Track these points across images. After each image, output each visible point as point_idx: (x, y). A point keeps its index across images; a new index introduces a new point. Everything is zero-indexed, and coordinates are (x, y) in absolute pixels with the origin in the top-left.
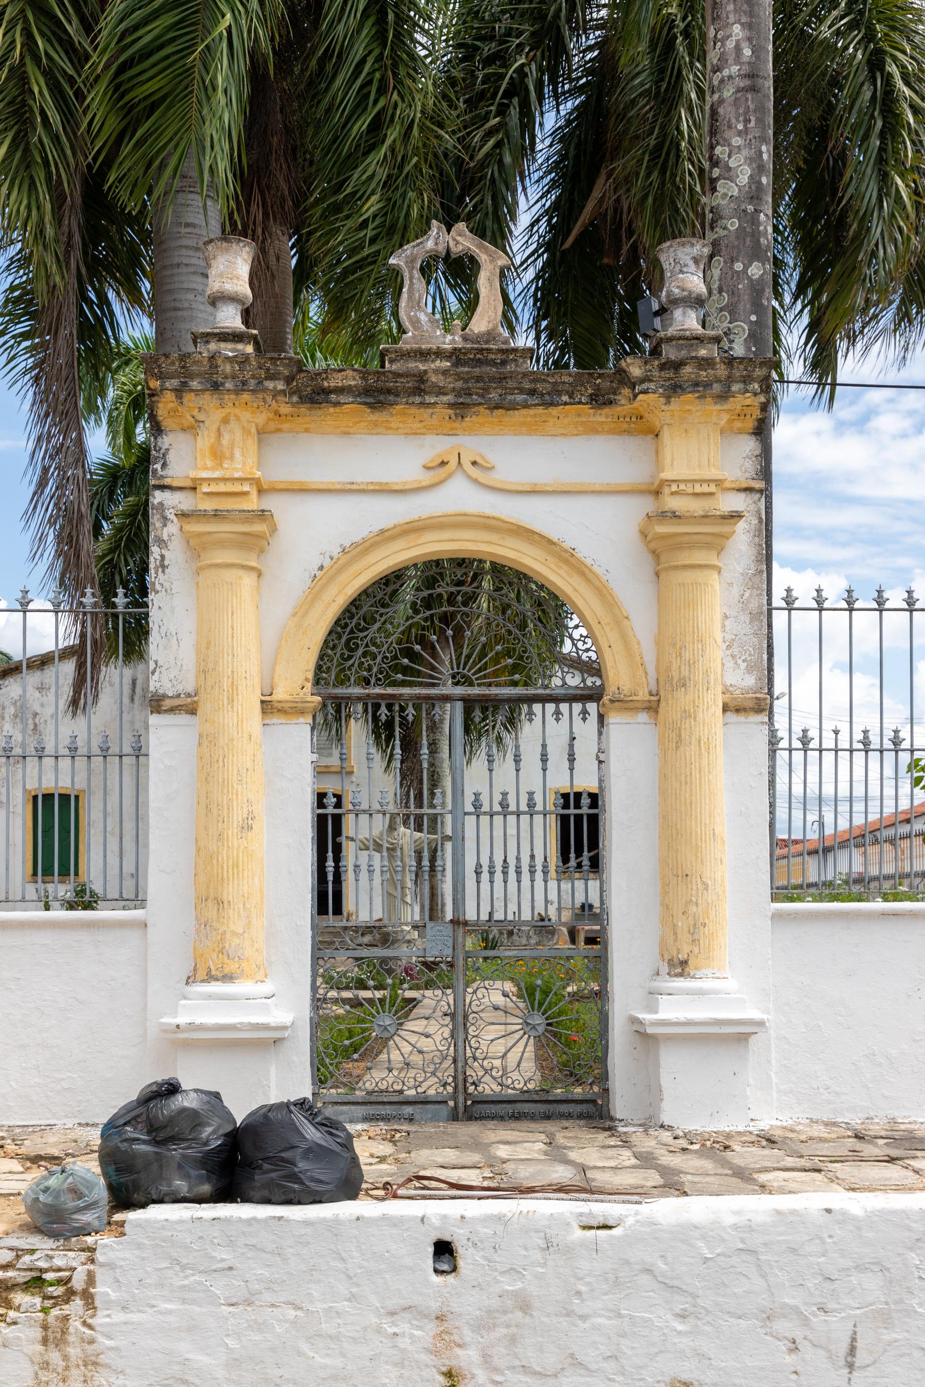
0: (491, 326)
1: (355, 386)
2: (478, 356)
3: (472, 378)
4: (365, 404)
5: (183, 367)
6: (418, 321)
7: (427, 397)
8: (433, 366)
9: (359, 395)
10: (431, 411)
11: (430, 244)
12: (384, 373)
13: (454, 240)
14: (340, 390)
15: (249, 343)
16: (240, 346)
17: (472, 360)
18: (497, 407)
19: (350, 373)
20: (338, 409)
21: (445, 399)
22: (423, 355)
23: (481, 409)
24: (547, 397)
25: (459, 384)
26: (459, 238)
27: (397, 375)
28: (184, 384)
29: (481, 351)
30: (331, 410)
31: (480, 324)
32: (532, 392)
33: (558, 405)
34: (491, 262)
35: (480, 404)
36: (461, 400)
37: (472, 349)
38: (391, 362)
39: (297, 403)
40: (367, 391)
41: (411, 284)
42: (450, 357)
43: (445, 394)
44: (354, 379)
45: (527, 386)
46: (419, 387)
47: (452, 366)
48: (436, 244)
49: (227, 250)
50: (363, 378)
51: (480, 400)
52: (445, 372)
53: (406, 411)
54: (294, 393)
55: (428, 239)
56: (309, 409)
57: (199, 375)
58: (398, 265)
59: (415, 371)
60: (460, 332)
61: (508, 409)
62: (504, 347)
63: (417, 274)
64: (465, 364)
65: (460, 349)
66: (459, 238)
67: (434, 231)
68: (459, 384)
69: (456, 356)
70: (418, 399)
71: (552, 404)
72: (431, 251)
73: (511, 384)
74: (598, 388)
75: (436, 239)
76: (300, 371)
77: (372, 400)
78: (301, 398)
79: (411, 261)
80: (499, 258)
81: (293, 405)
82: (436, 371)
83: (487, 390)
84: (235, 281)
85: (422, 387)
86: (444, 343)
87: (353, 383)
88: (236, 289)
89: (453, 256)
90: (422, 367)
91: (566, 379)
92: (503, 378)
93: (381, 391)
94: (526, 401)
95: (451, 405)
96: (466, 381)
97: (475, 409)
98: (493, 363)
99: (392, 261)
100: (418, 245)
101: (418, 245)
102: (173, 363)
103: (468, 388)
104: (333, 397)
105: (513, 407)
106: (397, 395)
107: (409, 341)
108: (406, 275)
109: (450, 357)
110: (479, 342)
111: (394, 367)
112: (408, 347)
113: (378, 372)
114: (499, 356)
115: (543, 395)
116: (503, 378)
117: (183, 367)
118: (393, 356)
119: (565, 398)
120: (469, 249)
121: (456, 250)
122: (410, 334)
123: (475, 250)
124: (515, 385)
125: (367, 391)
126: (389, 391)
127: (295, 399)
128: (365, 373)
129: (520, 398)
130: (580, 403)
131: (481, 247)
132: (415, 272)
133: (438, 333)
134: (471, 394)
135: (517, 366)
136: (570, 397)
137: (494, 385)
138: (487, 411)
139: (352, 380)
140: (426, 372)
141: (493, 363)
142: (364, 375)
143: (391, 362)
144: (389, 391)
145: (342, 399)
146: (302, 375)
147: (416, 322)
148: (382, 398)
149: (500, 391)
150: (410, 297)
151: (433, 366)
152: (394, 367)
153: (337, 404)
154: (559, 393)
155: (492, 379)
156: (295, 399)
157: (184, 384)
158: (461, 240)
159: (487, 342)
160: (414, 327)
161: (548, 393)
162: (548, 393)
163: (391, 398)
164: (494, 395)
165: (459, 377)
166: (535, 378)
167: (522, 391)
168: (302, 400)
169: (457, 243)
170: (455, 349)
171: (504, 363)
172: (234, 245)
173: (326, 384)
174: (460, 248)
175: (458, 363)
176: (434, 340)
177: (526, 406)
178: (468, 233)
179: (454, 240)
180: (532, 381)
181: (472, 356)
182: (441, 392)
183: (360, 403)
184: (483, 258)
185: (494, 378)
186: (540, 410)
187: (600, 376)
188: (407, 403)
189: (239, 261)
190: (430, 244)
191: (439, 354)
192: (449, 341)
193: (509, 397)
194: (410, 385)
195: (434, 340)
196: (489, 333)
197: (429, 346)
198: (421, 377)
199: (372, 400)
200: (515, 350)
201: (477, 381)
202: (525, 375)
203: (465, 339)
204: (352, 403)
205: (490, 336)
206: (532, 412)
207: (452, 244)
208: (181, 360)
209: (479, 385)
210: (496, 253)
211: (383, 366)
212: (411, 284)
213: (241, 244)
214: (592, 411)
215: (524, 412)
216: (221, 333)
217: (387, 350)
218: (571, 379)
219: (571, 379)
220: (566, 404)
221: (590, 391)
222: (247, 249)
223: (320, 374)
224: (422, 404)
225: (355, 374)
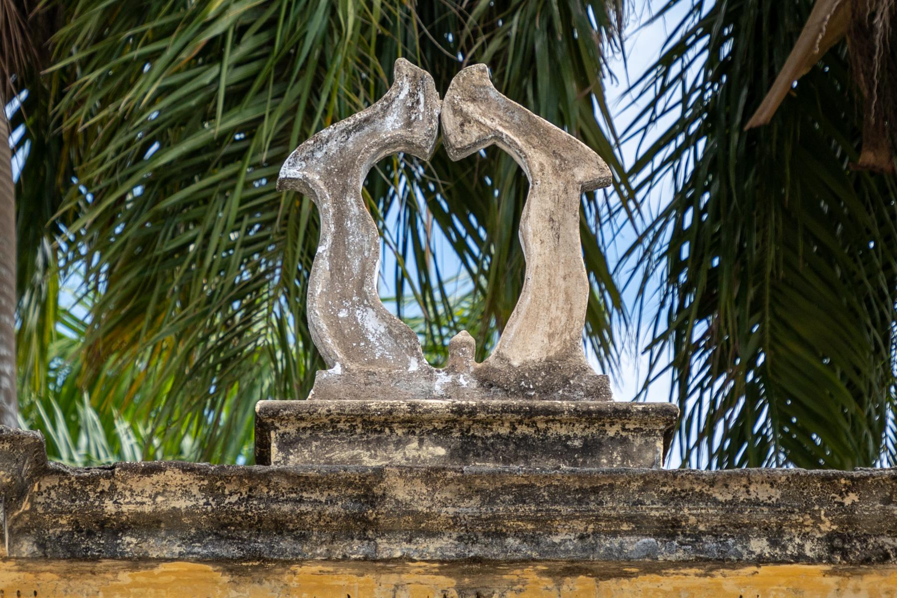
0: (557, 345)
1: (189, 512)
2: (522, 430)
3: (506, 489)
4: (216, 560)
6: (360, 334)
7: (382, 543)
8: (398, 457)
9: (200, 537)
10: (394, 579)
11: (391, 124)
12: (265, 477)
13: (458, 111)
14: (148, 525)
17: (506, 440)
18: (573, 570)
19: (174, 477)
20: (141, 576)
21: (432, 547)
22: (373, 426)
23: (530, 574)
24: (710, 544)
25: (471, 507)
26: (469, 108)
27: (302, 482)
29: (531, 413)
30: (125, 577)
31: (524, 342)
32: (669, 529)
33: (739, 563)
34: (556, 171)
35: (527, 561)
36: (476, 551)
37: (505, 409)
38: (286, 445)
39: (33, 558)
40: (221, 527)
41: (341, 232)
42: (445, 433)
43: (431, 534)
44: (186, 493)
45: (655, 511)
46: (363, 515)
47: (452, 456)
48: (409, 124)
50: (210, 491)
51: (527, 550)
52: (432, 475)
53: (328, 580)
54: (24, 531)
55: (385, 110)
56: (65, 575)
58: (305, 182)
59: (352, 472)
60: (473, 365)
61: (604, 576)
62: (593, 404)
63: (355, 206)
64: (487, 450)
65: (473, 412)
66: (469, 108)
67: (402, 90)
68: (471, 507)
69: (462, 430)
70: (357, 549)
71: (723, 562)
72: (394, 142)
73: (612, 506)
74: (848, 517)
75: (408, 111)
76: (42, 471)
77: (233, 551)
78: (42, 545)
79: (339, 171)
80: (579, 161)
81: (22, 563)
82: (407, 472)
83: (545, 523)
85: (371, 514)
86: (429, 394)
87: (182, 504)
89: (455, 156)
90: (369, 460)
91: (761, 492)
92: (590, 491)
93: (258, 526)
94: (651, 553)
95: (448, 565)
96: (489, 498)
97: (514, 575)
98: (561, 449)
99: (289, 171)
100: (358, 127)
101: (358, 127)
103: (495, 518)
104: (129, 541)
105: (617, 569)
106: (302, 538)
107: (335, 388)
108: (327, 209)
109: (445, 433)
110: (522, 392)
111: (294, 460)
112: (332, 404)
113: (250, 475)
114: (578, 430)
115: (697, 536)
116: (590, 491)
118: (291, 429)
119: (759, 545)
120: (498, 137)
121: (463, 140)
122: (337, 369)
123: (514, 140)
124: (622, 509)
125: (221, 527)
126: (280, 527)
127: (27, 547)
128: (214, 477)
129: (635, 544)
130: (800, 558)
131: (528, 130)
132: (350, 200)
133: (414, 366)
134: (501, 535)
135: (626, 456)
136: (773, 543)
137: (565, 510)
138: (547, 581)
139: (181, 496)
140: (379, 473)
141: (561, 449)
142: (214, 482)
143: (286, 445)
144: (280, 527)
145: (154, 547)
146: (47, 482)
147: (353, 339)
148: (260, 544)
149: (580, 526)
150: (337, 270)
151: (398, 457)
152: (294, 460)
153: (141, 561)
154: (743, 532)
155: (560, 494)
156: (27, 547)
158: (477, 111)
159: (546, 391)
160: (347, 351)
161: (714, 533)
162: (714, 533)
163: (286, 544)
164: (564, 537)
165: (469, 487)
166: (681, 488)
167: (640, 525)
168: (48, 550)
169: (466, 120)
170: (459, 410)
171: (591, 448)
173: (110, 507)
174: (474, 133)
175: (466, 449)
176: (402, 387)
177: (652, 566)
178: (494, 93)
179: (458, 111)
180: (668, 499)
181: (504, 431)
182: (421, 527)
183: (202, 560)
184: (536, 162)
185: (566, 490)
186: (691, 578)
187: (856, 484)
188: (328, 559)
190: (391, 124)
191: (415, 423)
192: (441, 390)
193: (607, 543)
194: (337, 509)
195: (402, 387)
196: (550, 365)
197: (388, 402)
198: (367, 489)
199: (233, 551)
200: (621, 413)
201: (520, 499)
202: (650, 481)
203: (486, 381)
204: (181, 558)
205: (556, 373)
206: (668, 582)
207: (450, 123)
209: (523, 509)
210: (570, 147)
211: (262, 457)
212: (341, 232)
214: (831, 581)
215: (647, 582)
217: (275, 414)
218: (776, 494)
219: (776, 494)
220: (760, 561)
221: (827, 526)
223: (93, 480)
224: (371, 562)
225: (188, 478)
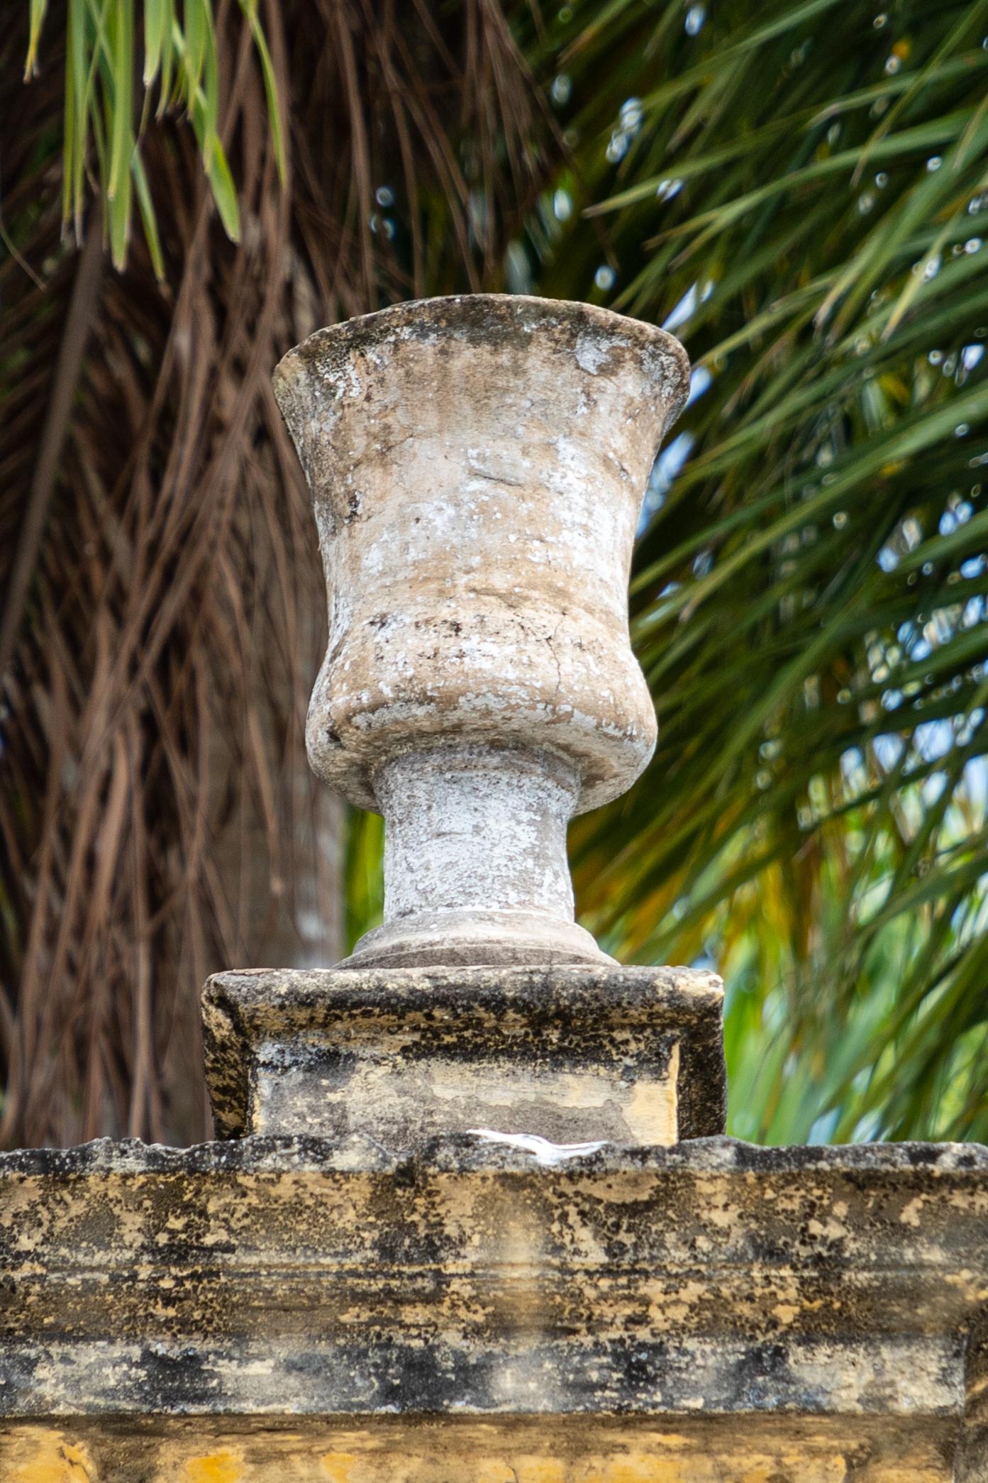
5: (177, 1253)
15: (653, 1063)
16: (581, 1090)
28: (176, 1378)
49: (484, 396)
57: (298, 1308)
84: (541, 615)
88: (545, 673)
102: (100, 1226)
117: (177, 1253)
157: (176, 1378)
172: (537, 360)
189: (573, 468)
208: (168, 1200)
213: (590, 354)
216: (444, 998)
222: (629, 384)
